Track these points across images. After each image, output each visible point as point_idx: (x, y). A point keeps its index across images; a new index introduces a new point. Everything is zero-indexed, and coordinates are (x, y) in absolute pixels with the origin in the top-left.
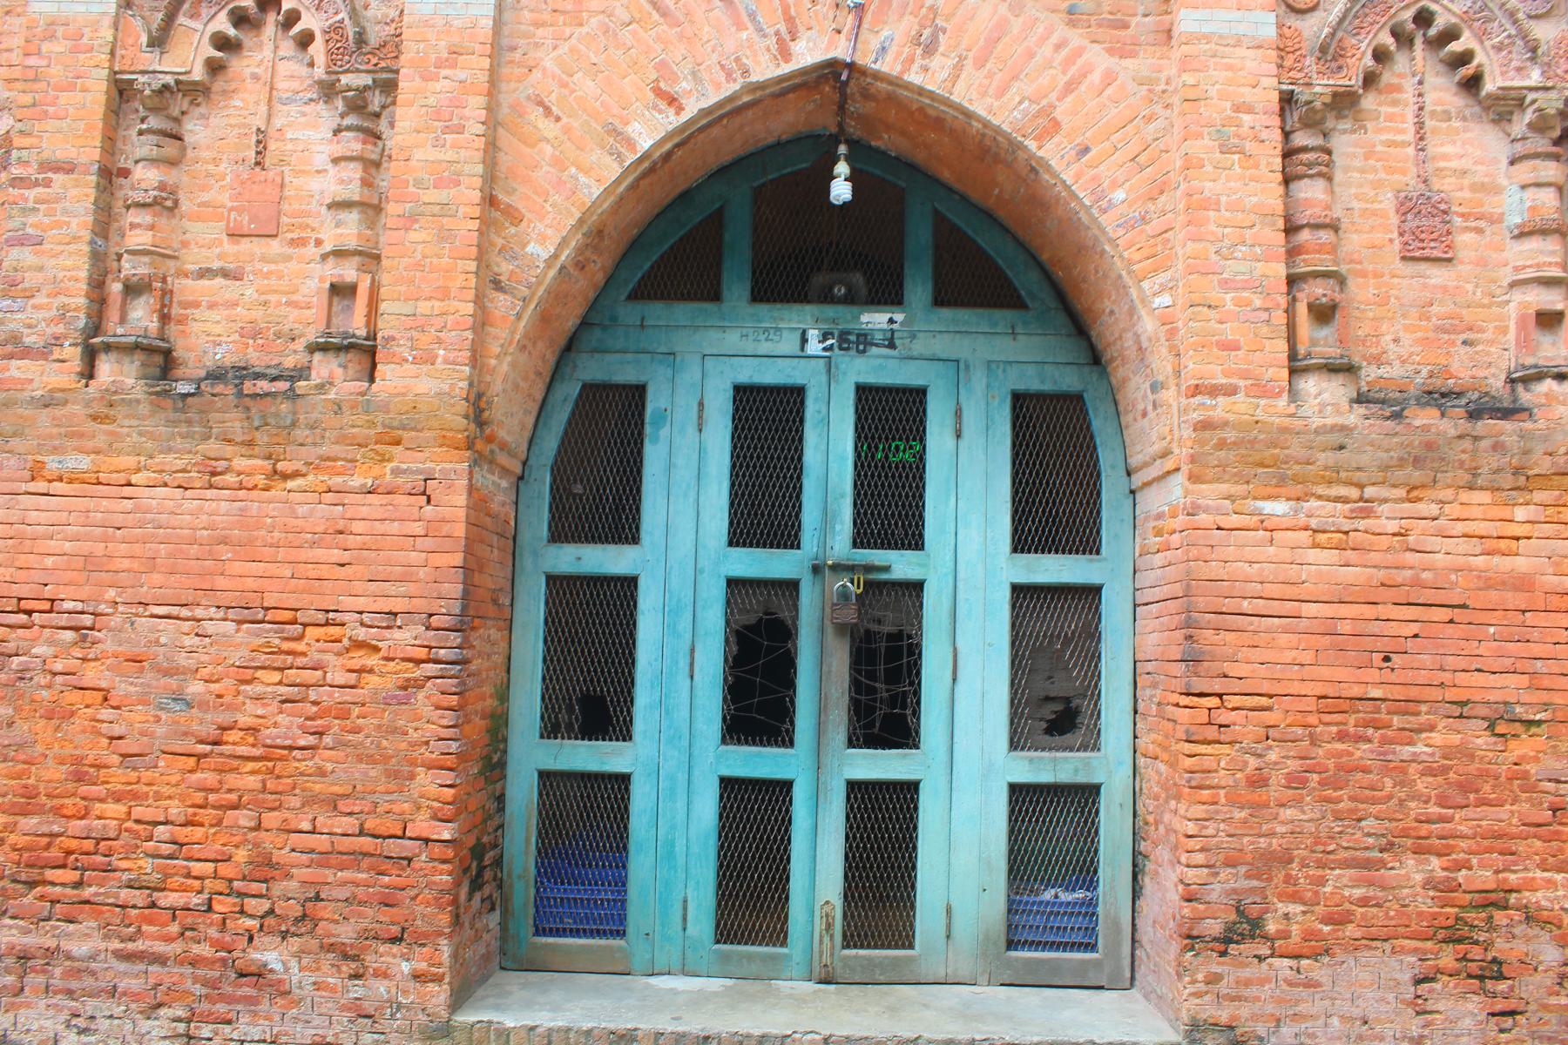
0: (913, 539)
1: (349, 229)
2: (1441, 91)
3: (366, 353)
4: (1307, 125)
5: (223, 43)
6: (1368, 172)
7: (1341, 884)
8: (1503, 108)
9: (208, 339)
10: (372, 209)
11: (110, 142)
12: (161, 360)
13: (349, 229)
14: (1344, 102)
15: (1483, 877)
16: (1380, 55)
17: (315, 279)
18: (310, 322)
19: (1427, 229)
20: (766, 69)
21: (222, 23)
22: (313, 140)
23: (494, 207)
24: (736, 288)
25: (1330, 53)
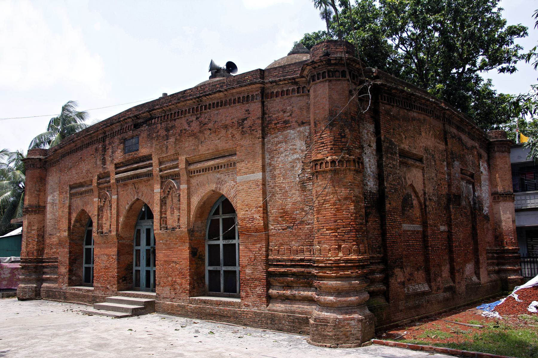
0: (140, 245)
5: (104, 202)
7: (165, 280)
11: (98, 212)
12: (102, 233)
15: (174, 279)
16: (169, 192)
20: (133, 200)
21: (104, 200)
24: (146, 218)
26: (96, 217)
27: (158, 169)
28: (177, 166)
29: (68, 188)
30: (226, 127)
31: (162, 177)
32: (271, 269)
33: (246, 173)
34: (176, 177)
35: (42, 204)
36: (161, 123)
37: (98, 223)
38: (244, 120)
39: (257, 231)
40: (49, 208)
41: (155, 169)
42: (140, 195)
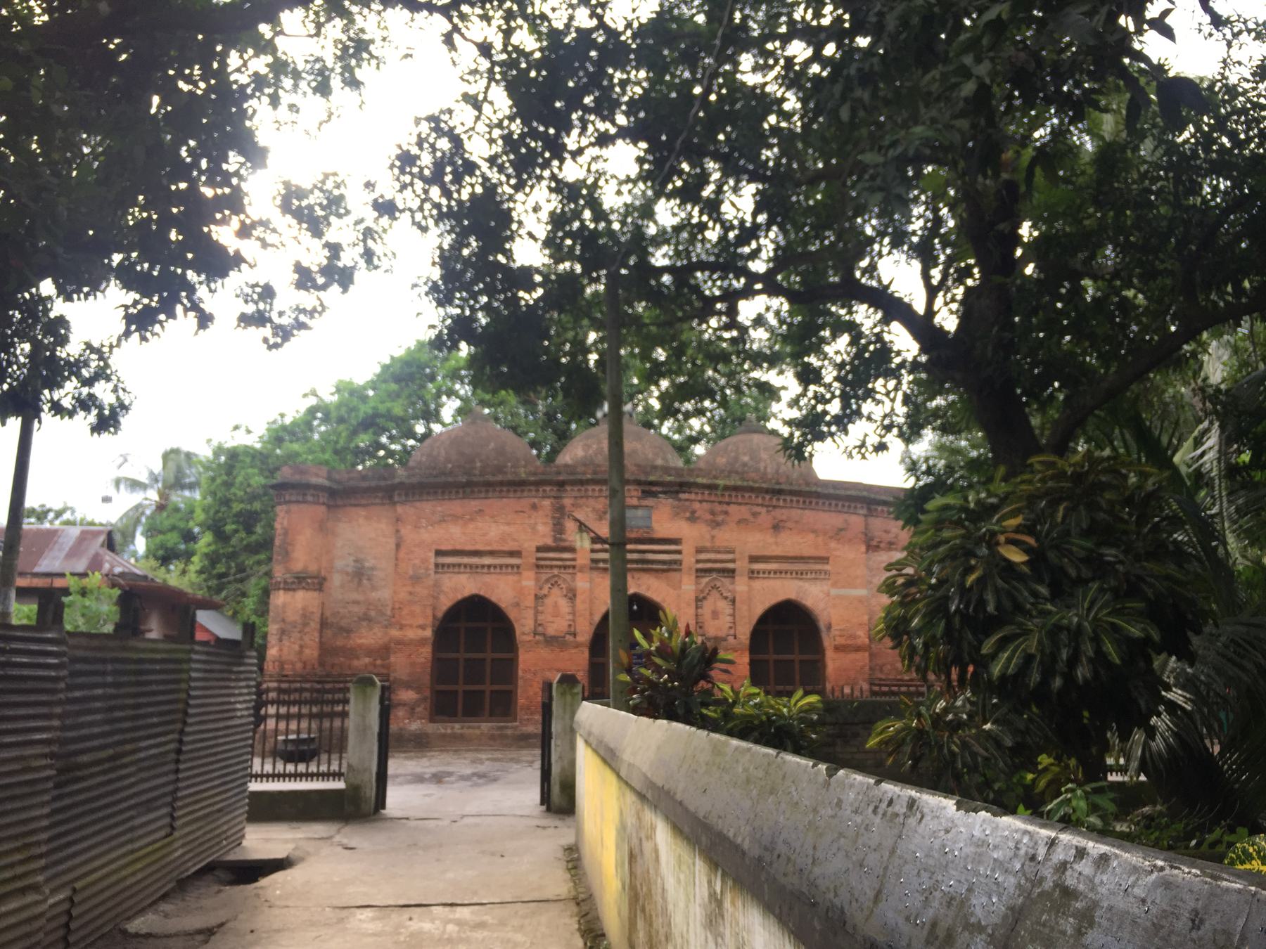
1: (571, 617)
2: (718, 595)
3: (575, 635)
4: (699, 601)
6: (707, 607)
8: (726, 598)
9: (551, 630)
10: (574, 613)
13: (571, 617)
14: (704, 598)
17: (567, 623)
18: (566, 629)
19: (715, 614)
22: (564, 604)
23: (591, 614)
25: (702, 591)
26: (531, 612)
27: (693, 560)
28: (733, 561)
29: (432, 554)
30: (814, 531)
31: (697, 570)
32: (876, 688)
33: (843, 587)
34: (731, 573)
35: (323, 573)
36: (701, 502)
37: (536, 621)
38: (841, 530)
39: (858, 649)
40: (336, 580)
41: (688, 558)
42: (644, 587)
